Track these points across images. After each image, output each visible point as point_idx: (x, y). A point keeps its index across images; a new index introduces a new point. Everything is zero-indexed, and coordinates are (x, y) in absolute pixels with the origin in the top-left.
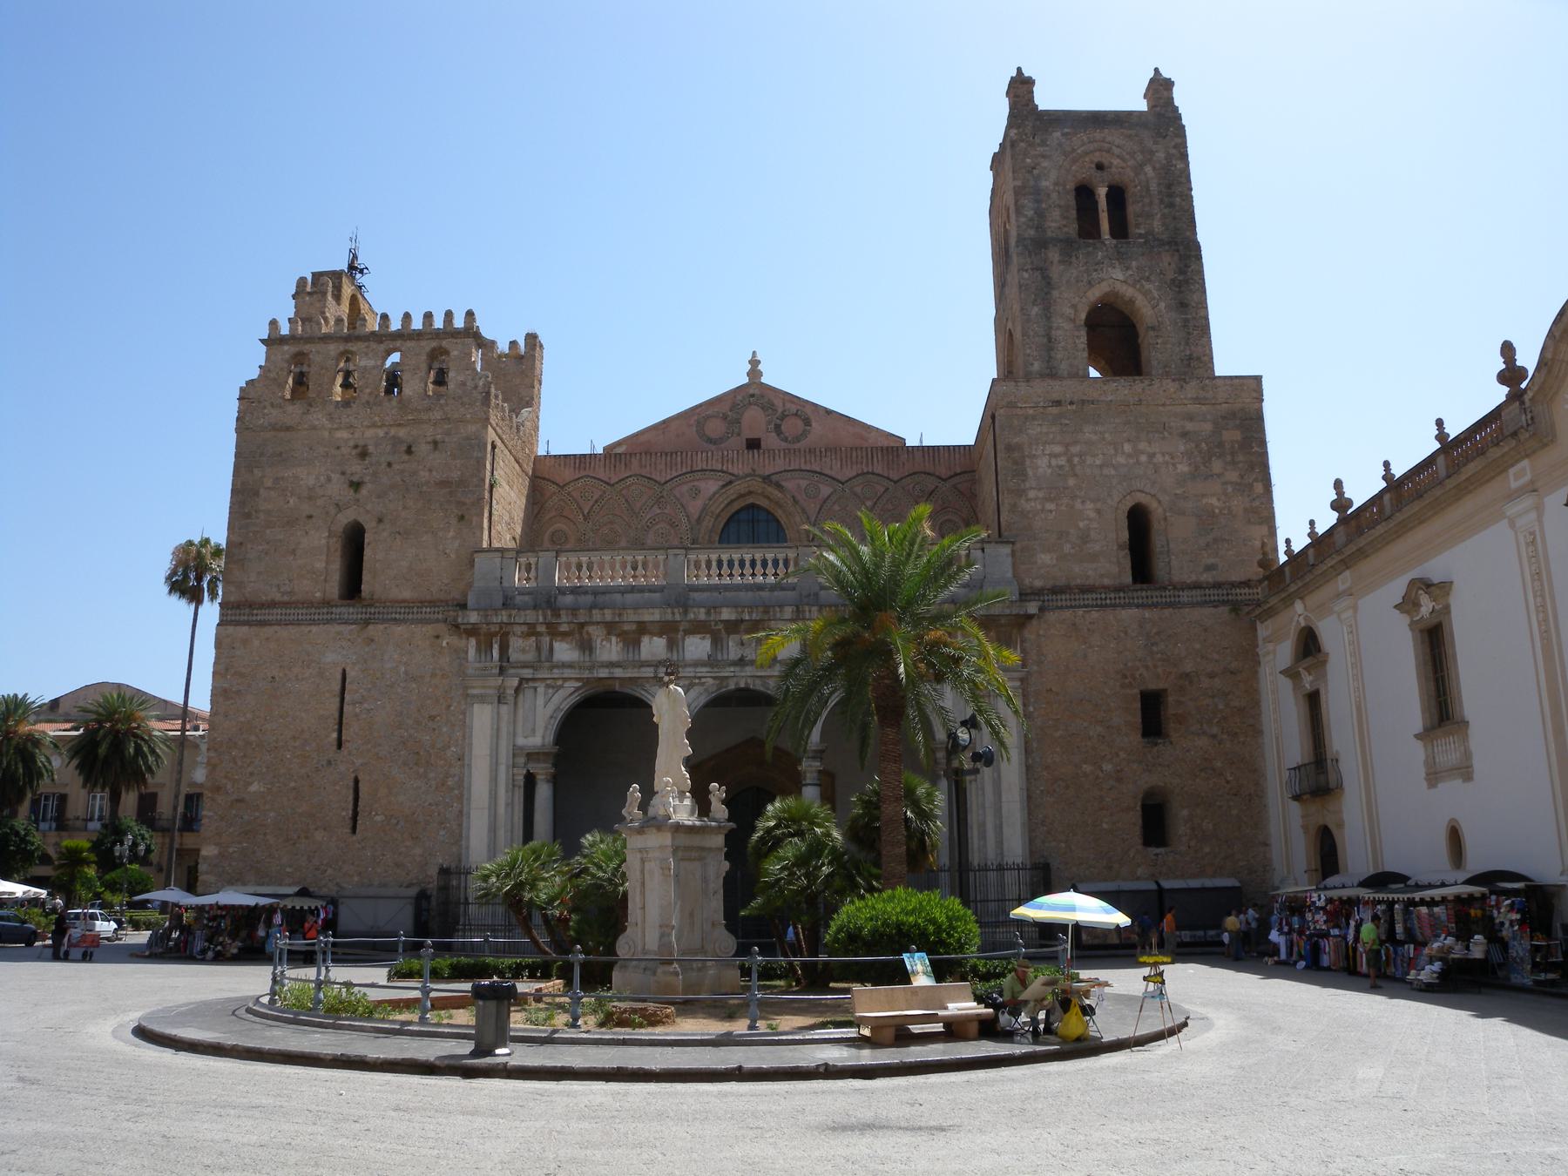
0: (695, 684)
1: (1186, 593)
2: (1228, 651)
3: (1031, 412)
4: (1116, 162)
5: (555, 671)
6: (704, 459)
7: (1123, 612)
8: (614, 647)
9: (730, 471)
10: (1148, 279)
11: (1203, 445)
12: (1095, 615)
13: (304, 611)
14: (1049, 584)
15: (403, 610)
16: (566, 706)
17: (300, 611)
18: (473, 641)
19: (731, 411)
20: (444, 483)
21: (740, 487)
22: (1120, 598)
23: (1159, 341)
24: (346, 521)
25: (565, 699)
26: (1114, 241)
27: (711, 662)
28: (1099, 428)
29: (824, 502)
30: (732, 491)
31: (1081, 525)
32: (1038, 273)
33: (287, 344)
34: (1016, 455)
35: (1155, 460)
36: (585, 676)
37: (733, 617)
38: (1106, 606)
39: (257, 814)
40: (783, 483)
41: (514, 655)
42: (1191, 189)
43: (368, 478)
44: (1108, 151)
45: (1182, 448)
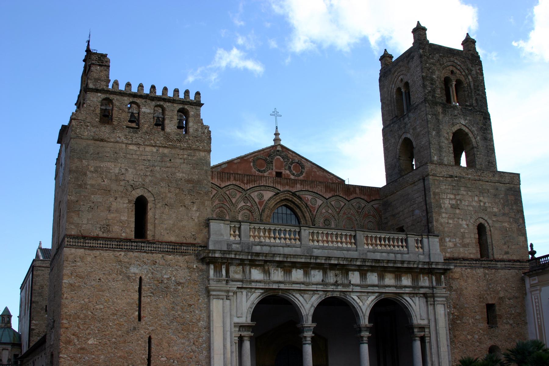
0: (315, 294)
1: (499, 263)
2: (514, 288)
3: (441, 179)
4: (458, 72)
5: (253, 284)
6: (265, 180)
7: (478, 270)
9: (277, 188)
10: (473, 125)
11: (502, 201)
12: (469, 270)
15: (171, 247)
16: (256, 302)
17: (114, 243)
18: (212, 267)
19: (268, 157)
20: (189, 181)
21: (282, 196)
22: (477, 263)
23: (478, 153)
24: (137, 196)
25: (256, 299)
26: (460, 107)
27: (323, 283)
29: (319, 208)
30: (278, 198)
32: (434, 117)
33: (100, 92)
34: (437, 197)
35: (486, 205)
36: (267, 287)
37: (336, 262)
39: (93, 356)
40: (301, 196)
41: (231, 274)
42: (485, 89)
43: (149, 173)
44: (455, 67)
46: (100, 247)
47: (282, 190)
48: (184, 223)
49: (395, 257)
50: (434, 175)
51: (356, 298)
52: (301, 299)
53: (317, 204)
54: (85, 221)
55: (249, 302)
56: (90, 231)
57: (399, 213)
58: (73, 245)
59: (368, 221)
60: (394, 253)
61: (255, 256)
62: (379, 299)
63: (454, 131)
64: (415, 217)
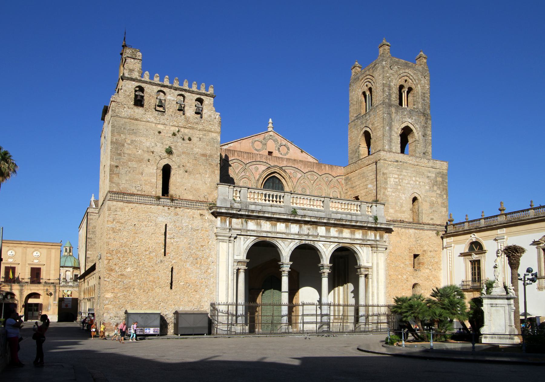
3: (390, 163)
5: (248, 232)
8: (268, 226)
13: (148, 199)
14: (392, 219)
16: (250, 245)
18: (219, 218)
20: (204, 155)
21: (272, 170)
23: (419, 145)
28: (407, 171)
31: (401, 201)
34: (385, 176)
35: (420, 184)
37: (309, 219)
38: (406, 227)
45: (427, 181)
46: (136, 201)
47: (272, 165)
48: (199, 186)
49: (352, 217)
50: (385, 160)
51: (322, 246)
52: (282, 244)
53: (297, 177)
54: (124, 182)
55: (246, 245)
56: (128, 189)
57: (356, 186)
58: (114, 199)
59: (334, 190)
60: (351, 215)
61: (251, 212)
62: (338, 247)
63: (402, 128)
64: (367, 190)
